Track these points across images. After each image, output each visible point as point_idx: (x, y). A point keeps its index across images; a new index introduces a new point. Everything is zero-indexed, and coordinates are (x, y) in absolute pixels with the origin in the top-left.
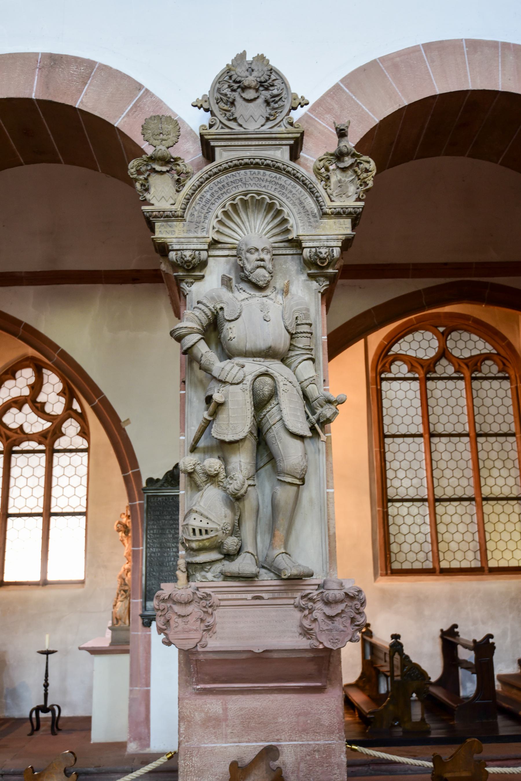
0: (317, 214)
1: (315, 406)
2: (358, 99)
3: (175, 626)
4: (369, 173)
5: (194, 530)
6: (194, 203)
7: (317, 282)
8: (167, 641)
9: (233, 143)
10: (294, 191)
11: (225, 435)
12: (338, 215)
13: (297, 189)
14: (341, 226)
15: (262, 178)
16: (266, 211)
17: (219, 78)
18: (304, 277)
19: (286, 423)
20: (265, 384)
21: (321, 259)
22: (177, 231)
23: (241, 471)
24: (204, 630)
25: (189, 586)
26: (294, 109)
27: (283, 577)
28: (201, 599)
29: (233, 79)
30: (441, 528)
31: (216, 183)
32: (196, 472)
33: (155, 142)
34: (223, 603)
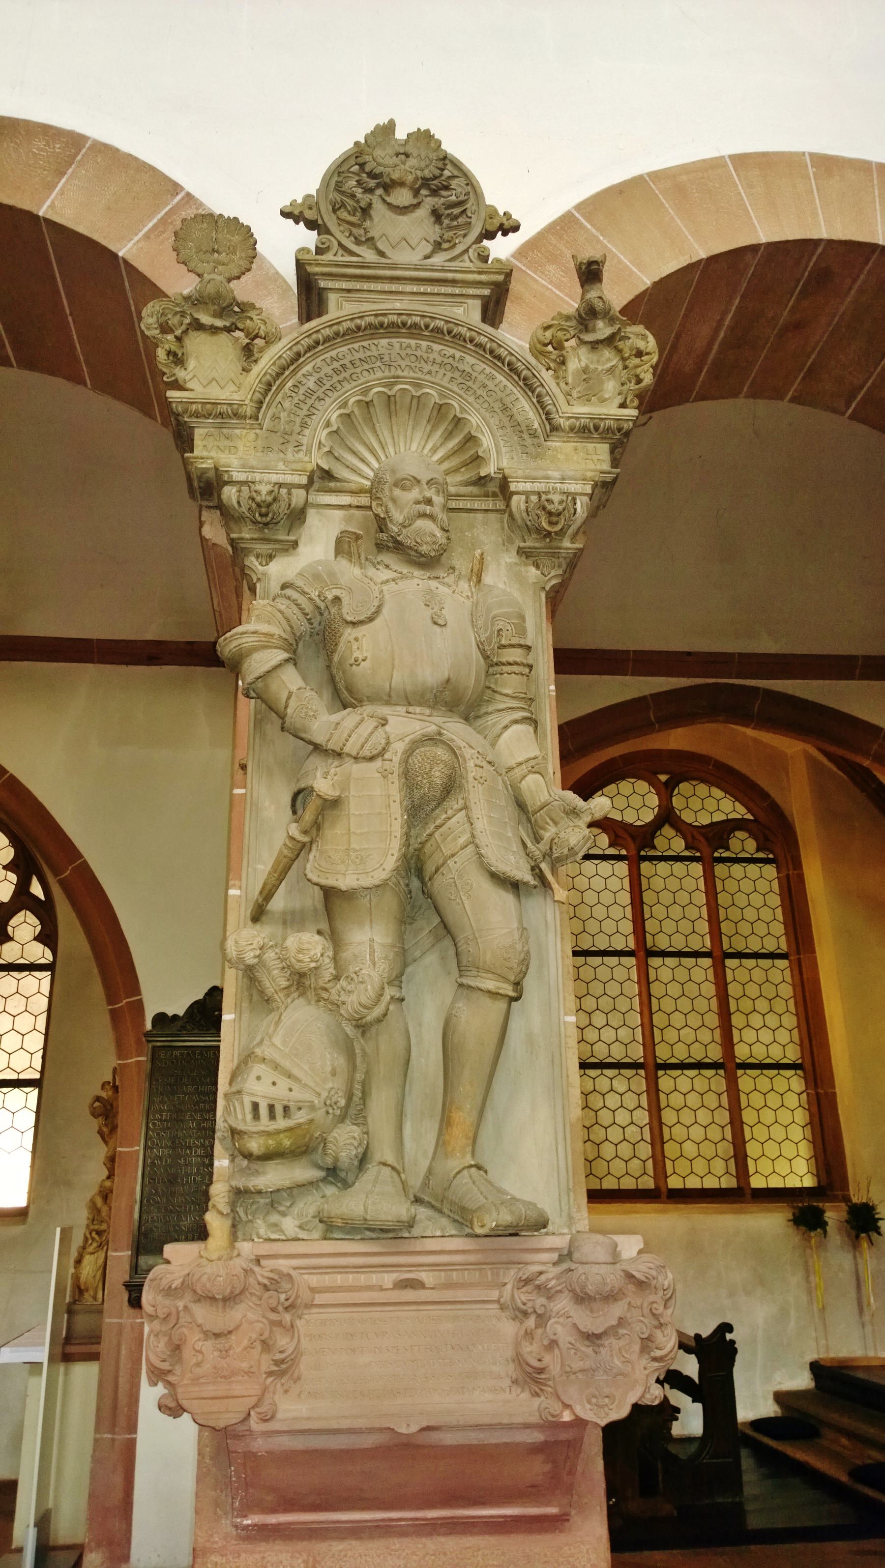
0: (539, 430)
1: (540, 823)
2: (608, 242)
3: (194, 1361)
4: (645, 358)
5: (255, 1106)
6: (280, 395)
7: (537, 567)
8: (173, 1405)
9: (366, 286)
10: (491, 385)
11: (339, 877)
13: (497, 381)
14: (589, 457)
15: (425, 358)
16: (432, 422)
17: (340, 166)
18: (510, 558)
19: (483, 852)
20: (434, 761)
21: (550, 514)
22: (241, 448)
23: (374, 964)
24: (270, 1374)
25: (235, 1253)
26: (490, 236)
27: (479, 1231)
28: (266, 1288)
29: (367, 169)
30: (668, 1116)
31: (328, 361)
32: (264, 966)
33: (201, 267)
34: (319, 1299)
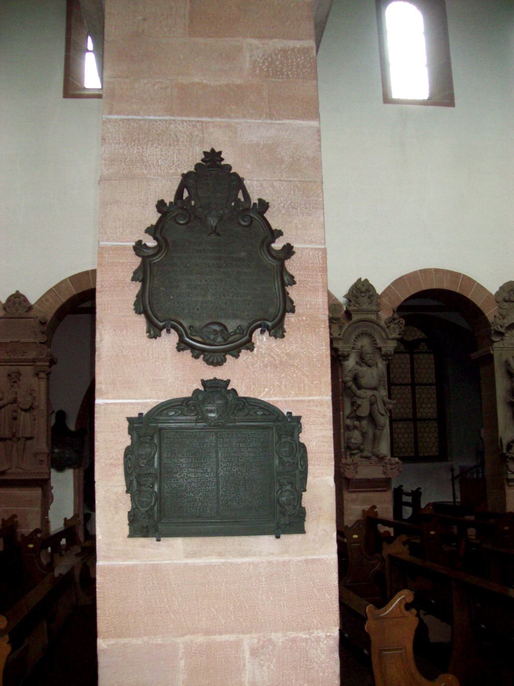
12: (393, 339)
